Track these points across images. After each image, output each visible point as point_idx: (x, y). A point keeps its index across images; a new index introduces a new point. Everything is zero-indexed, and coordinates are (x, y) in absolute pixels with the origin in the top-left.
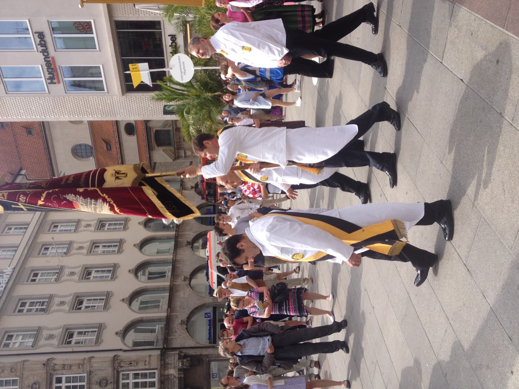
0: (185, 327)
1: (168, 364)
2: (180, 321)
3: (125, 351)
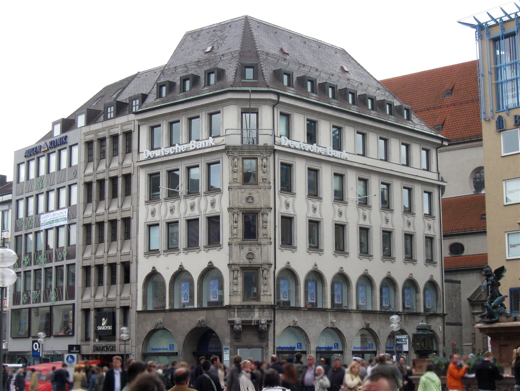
0: (291, 325)
1: (263, 311)
2: (296, 320)
3: (274, 272)
